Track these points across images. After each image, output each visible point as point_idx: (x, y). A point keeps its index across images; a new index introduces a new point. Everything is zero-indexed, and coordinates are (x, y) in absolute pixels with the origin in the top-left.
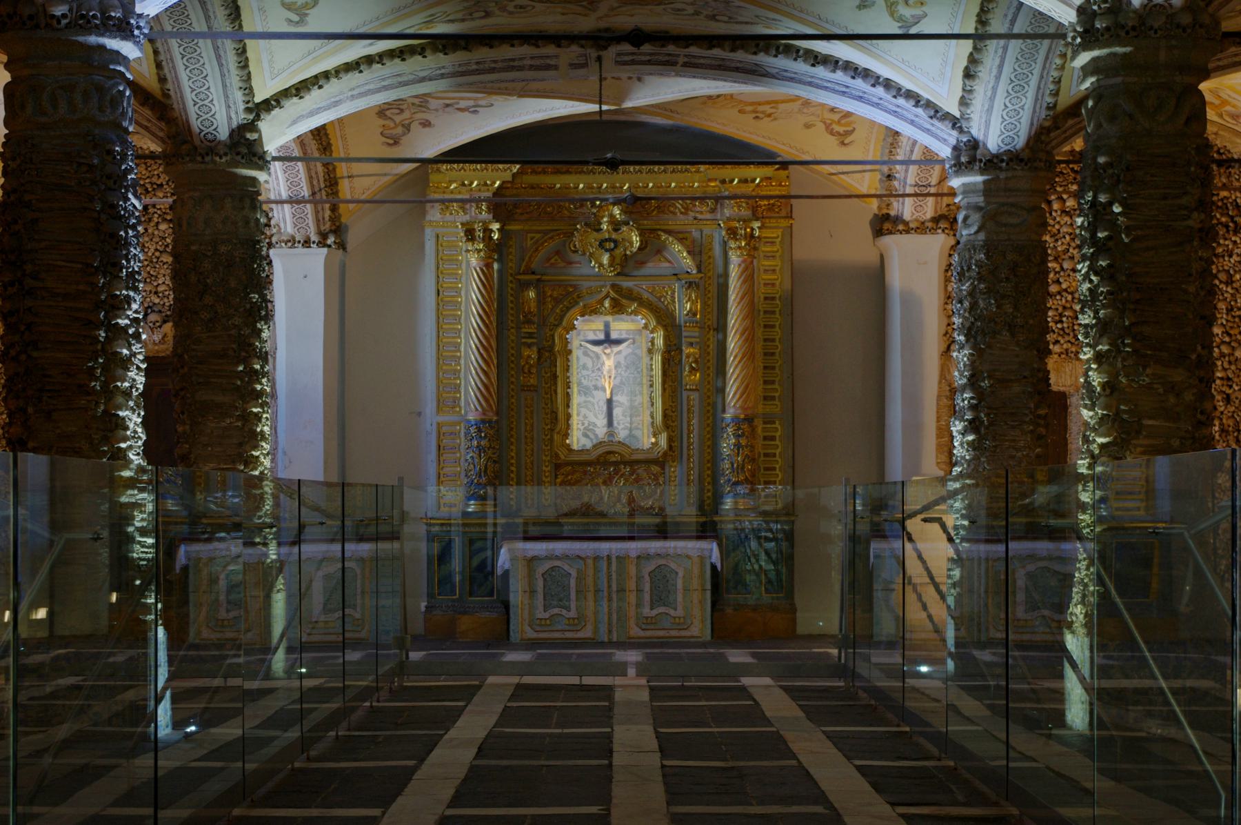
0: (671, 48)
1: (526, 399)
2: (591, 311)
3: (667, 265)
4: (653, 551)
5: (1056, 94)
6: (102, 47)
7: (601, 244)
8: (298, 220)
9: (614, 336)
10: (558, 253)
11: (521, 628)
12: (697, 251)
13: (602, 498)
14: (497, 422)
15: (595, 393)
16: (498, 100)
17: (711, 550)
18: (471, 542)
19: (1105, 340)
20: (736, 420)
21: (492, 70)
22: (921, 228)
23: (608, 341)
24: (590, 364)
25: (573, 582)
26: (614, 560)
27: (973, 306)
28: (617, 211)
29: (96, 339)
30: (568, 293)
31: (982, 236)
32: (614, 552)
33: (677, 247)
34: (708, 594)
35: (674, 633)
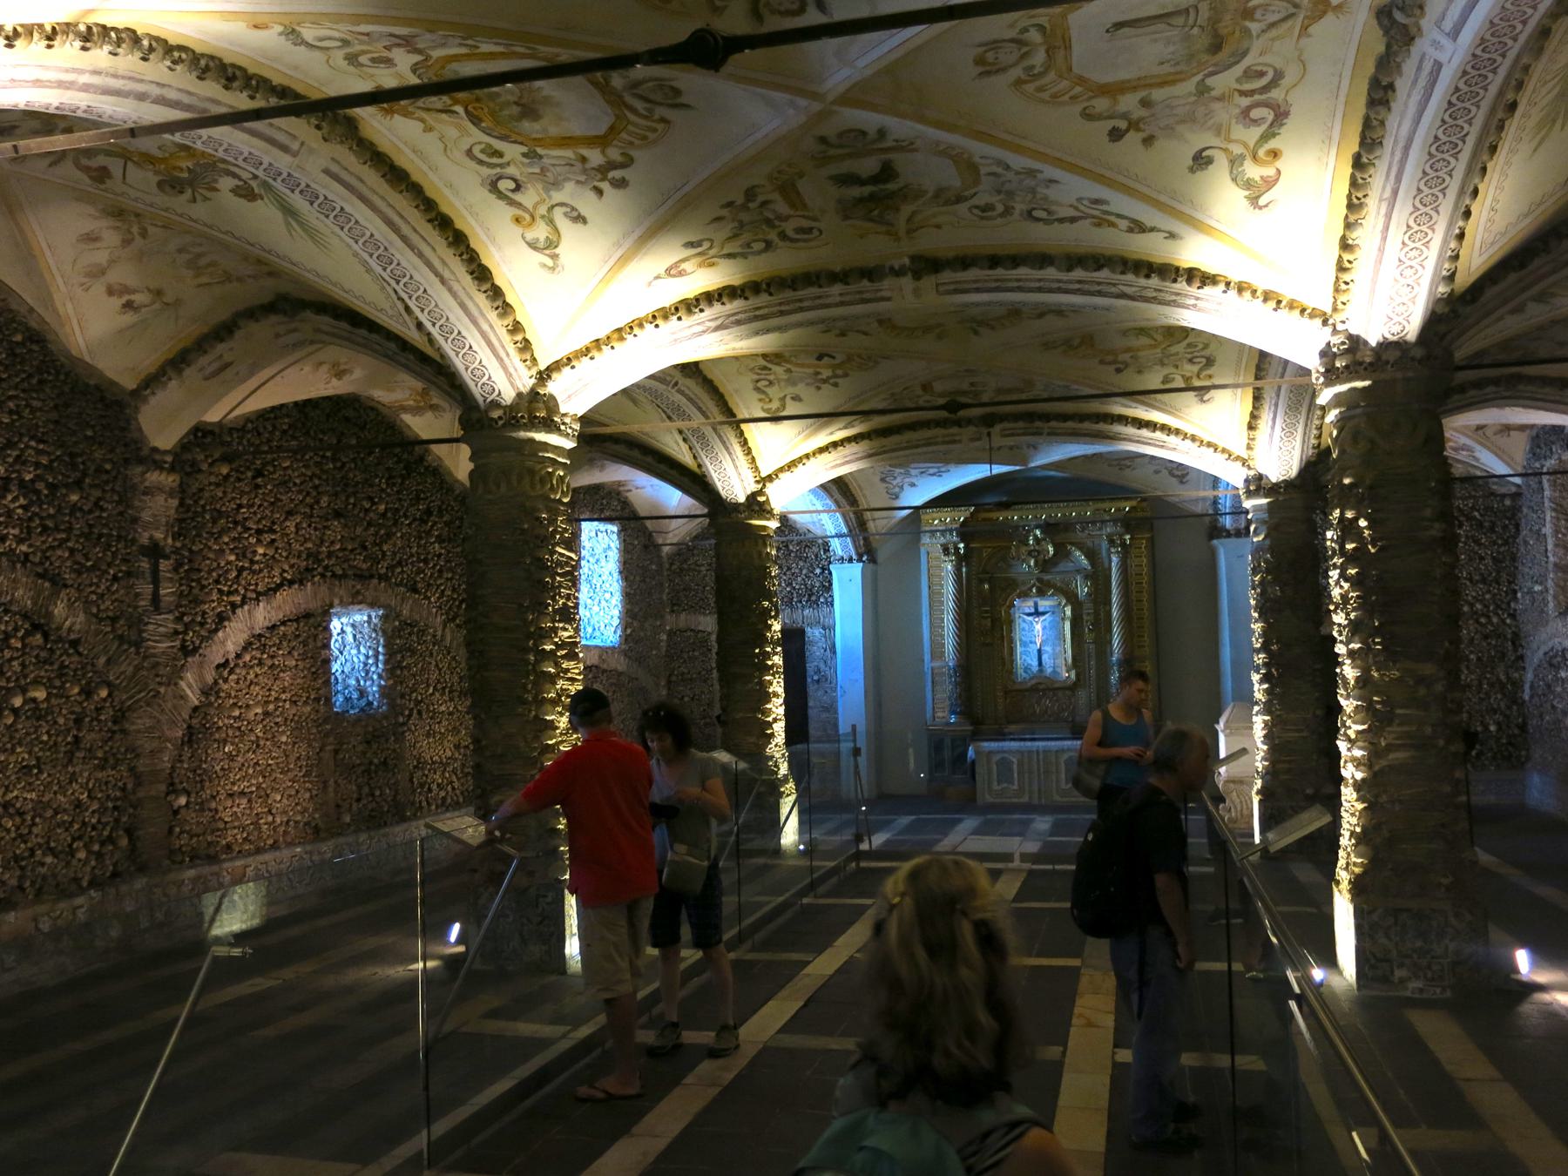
0: (1038, 424)
2: (1025, 595)
5: (1319, 437)
6: (532, 441)
8: (844, 547)
12: (1091, 555)
16: (952, 467)
19: (1357, 638)
20: (1118, 660)
21: (917, 446)
23: (1037, 613)
25: (1015, 767)
27: (1262, 594)
28: (1038, 532)
29: (527, 662)
31: (1268, 542)
33: (1078, 553)
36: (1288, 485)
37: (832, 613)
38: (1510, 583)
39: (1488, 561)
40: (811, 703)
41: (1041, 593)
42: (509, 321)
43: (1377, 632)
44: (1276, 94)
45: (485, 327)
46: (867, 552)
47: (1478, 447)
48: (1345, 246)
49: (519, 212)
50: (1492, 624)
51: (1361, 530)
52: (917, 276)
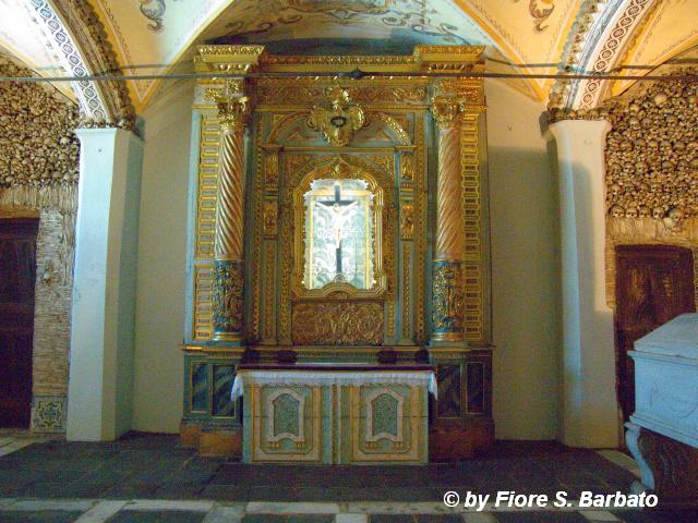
1: (268, 247)
2: (324, 175)
3: (387, 140)
4: (376, 381)
9: (342, 198)
10: (297, 129)
13: (331, 331)
14: (241, 264)
15: (328, 245)
17: (430, 380)
18: (215, 368)
20: (445, 263)
22: (588, 116)
23: (338, 201)
24: (323, 223)
26: (339, 390)
28: (346, 94)
30: (305, 162)
32: (339, 381)
34: (426, 420)
35: (394, 457)
37: (75, 192)
40: (38, 310)
41: (346, 174)
46: (128, 120)
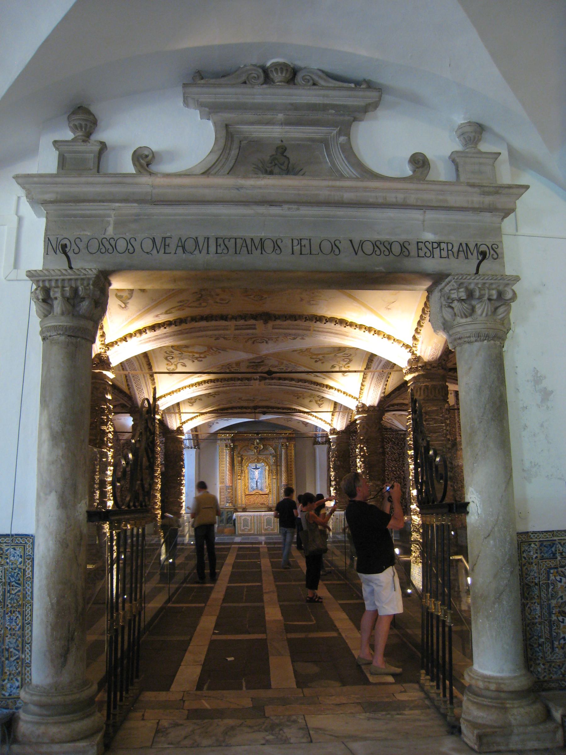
7: (255, 448)
8: (190, 443)
9: (258, 467)
11: (238, 531)
12: (275, 449)
18: (227, 512)
22: (323, 443)
23: (256, 468)
31: (336, 448)
36: (342, 432)
38: (403, 461)
39: (396, 454)
41: (258, 461)
42: (154, 387)
43: (368, 474)
44: (349, 357)
45: (148, 387)
47: (393, 419)
48: (362, 385)
49: (169, 363)
50: (397, 474)
51: (364, 450)
52: (260, 380)
